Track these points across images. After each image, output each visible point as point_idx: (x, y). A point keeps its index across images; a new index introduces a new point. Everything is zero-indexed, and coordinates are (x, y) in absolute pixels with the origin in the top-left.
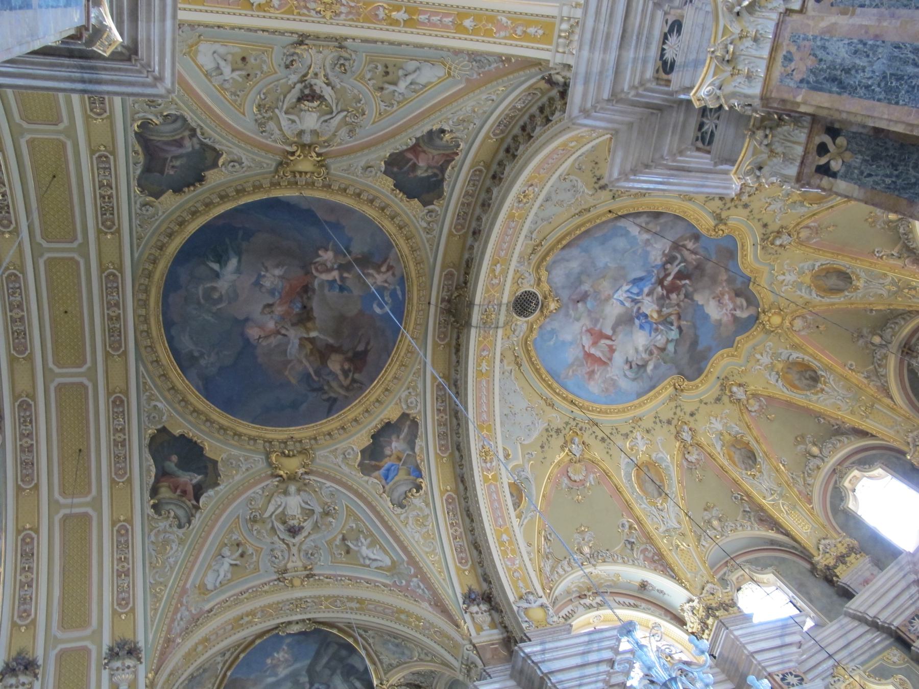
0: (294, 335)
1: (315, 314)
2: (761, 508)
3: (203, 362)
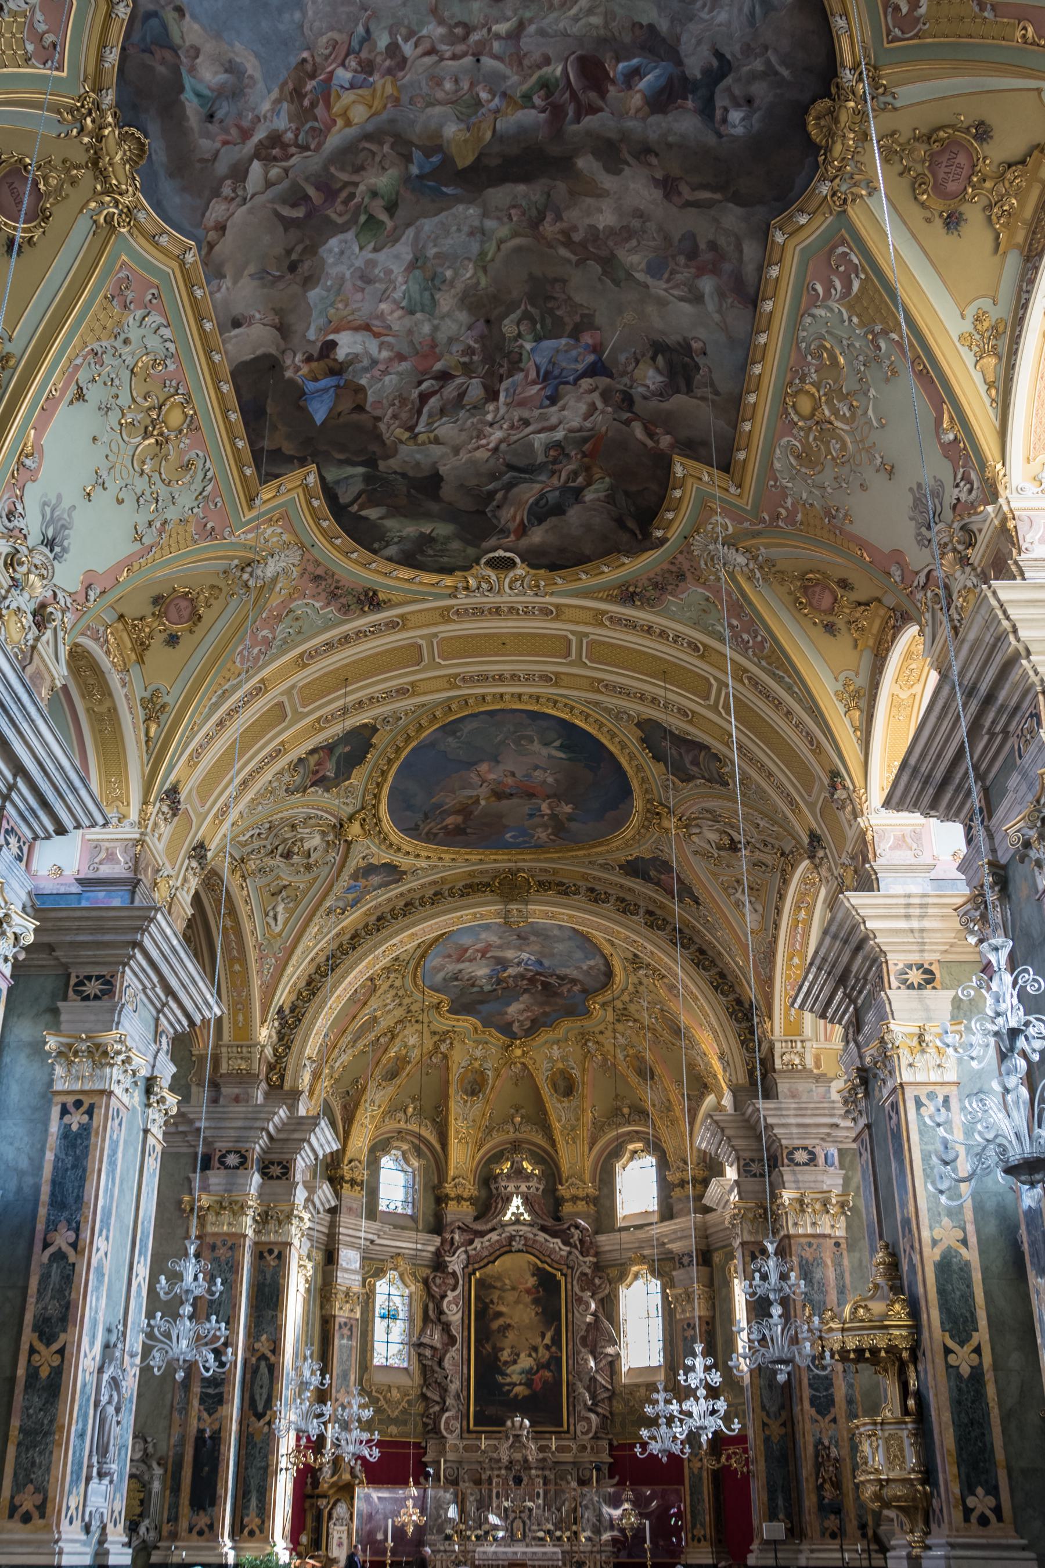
0: (483, 791)
1: (505, 802)
3: (450, 739)
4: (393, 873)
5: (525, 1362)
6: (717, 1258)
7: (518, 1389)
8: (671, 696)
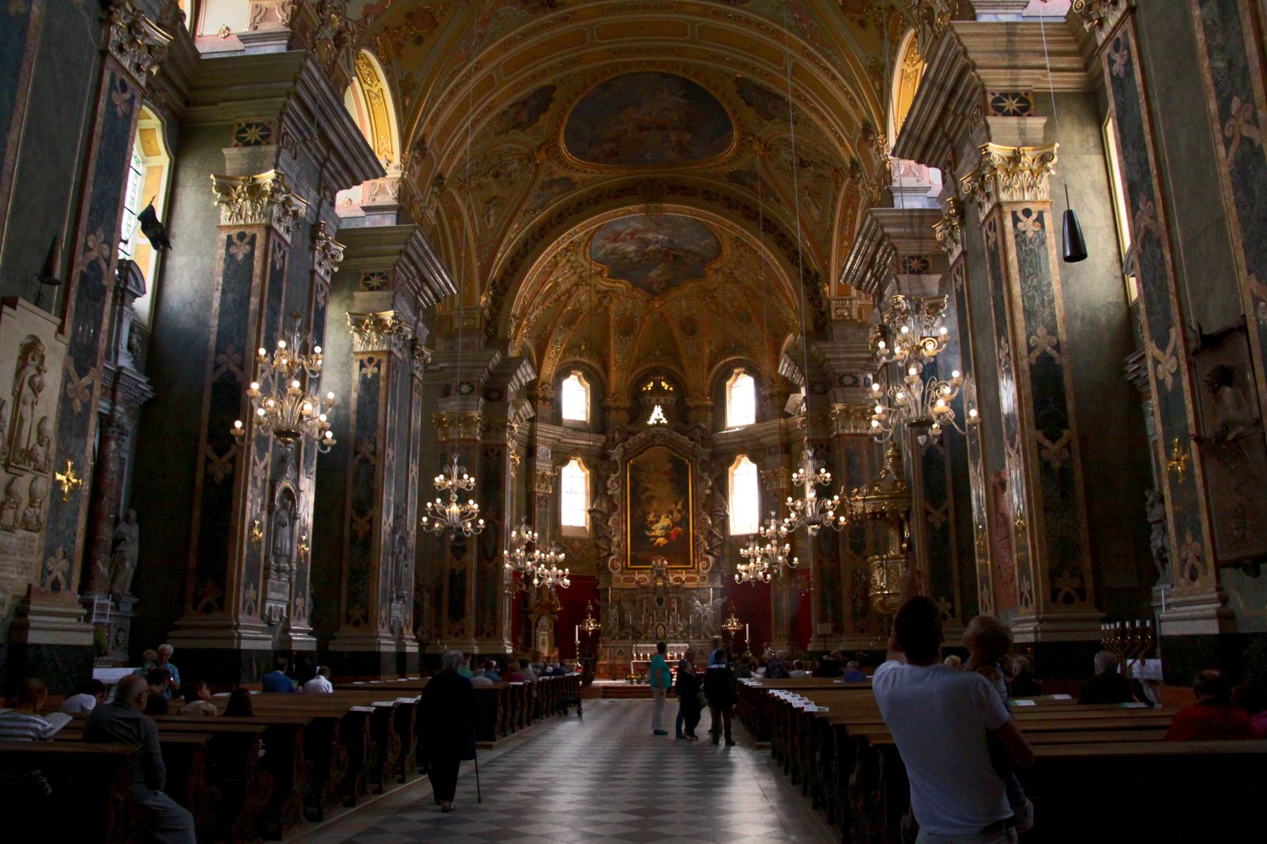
2: (546, 344)
4: (569, 184)
5: (665, 521)
6: (794, 448)
7: (660, 540)
8: (757, 64)
